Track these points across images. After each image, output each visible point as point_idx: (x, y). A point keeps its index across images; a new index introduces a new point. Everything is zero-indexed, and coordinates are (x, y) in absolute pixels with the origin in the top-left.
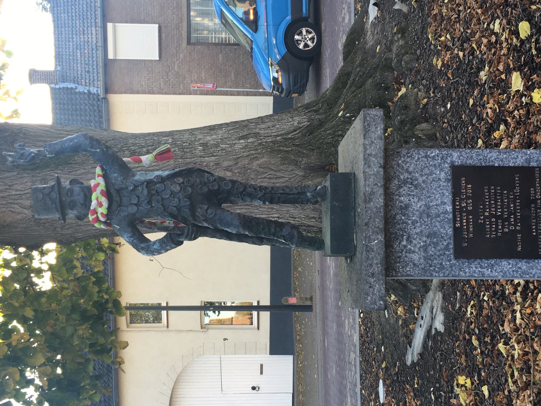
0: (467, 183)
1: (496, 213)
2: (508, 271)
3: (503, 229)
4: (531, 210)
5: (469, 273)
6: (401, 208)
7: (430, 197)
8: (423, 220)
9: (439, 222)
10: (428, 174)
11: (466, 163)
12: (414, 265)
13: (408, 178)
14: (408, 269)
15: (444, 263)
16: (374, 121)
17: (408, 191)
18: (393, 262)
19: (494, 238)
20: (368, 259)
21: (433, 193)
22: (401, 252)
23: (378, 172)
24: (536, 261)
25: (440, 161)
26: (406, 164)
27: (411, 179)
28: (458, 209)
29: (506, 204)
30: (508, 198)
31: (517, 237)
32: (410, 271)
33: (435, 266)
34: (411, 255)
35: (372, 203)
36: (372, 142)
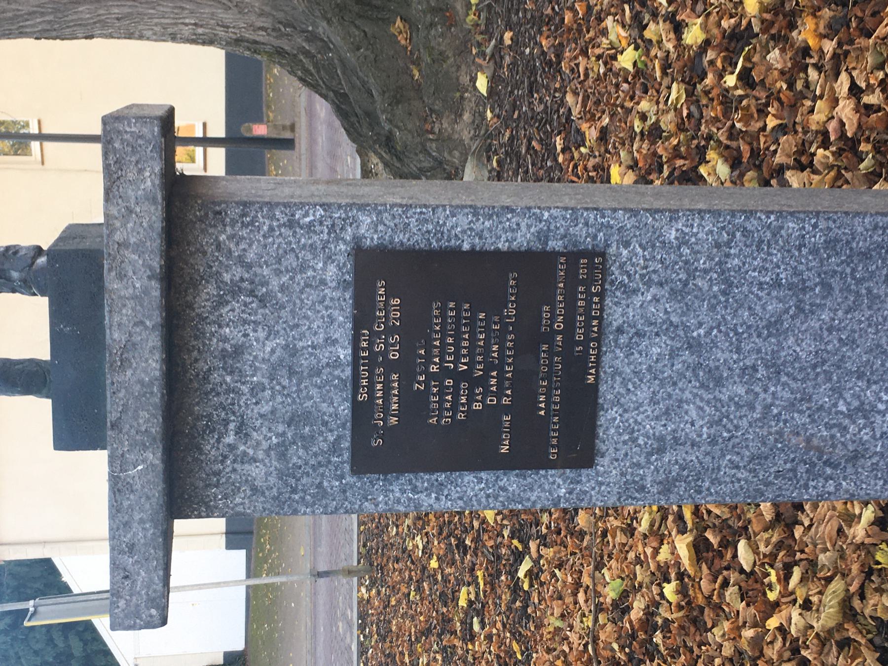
0: (389, 295)
1: (456, 367)
2: (476, 495)
3: (469, 402)
4: (538, 359)
5: (386, 503)
6: (224, 355)
7: (297, 326)
8: (279, 384)
9: (320, 388)
10: (294, 270)
11: (391, 242)
12: (255, 490)
13: (242, 280)
14: (238, 500)
15: (325, 484)
16: (134, 152)
17: (243, 311)
18: (201, 484)
19: (447, 427)
20: (118, 511)
21: (306, 317)
22: (222, 462)
23: (146, 291)
24: (542, 472)
25: (326, 237)
26: (237, 244)
27: (252, 282)
28: (364, 358)
29: (481, 343)
30: (487, 330)
31: (501, 422)
32: (242, 504)
33: (304, 491)
34: (247, 467)
35: (129, 373)
36: (130, 211)
